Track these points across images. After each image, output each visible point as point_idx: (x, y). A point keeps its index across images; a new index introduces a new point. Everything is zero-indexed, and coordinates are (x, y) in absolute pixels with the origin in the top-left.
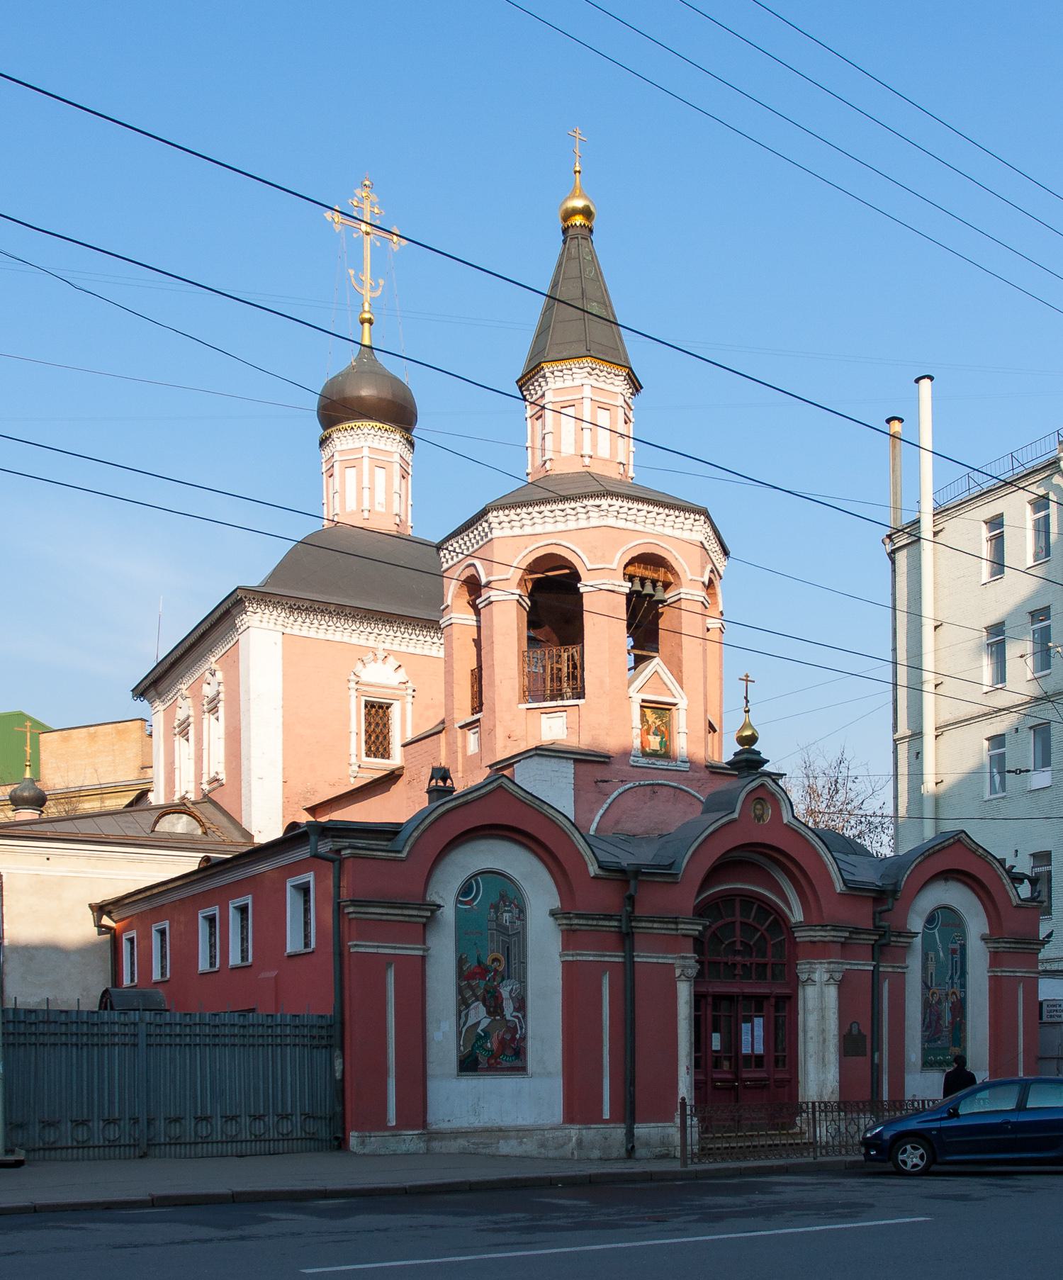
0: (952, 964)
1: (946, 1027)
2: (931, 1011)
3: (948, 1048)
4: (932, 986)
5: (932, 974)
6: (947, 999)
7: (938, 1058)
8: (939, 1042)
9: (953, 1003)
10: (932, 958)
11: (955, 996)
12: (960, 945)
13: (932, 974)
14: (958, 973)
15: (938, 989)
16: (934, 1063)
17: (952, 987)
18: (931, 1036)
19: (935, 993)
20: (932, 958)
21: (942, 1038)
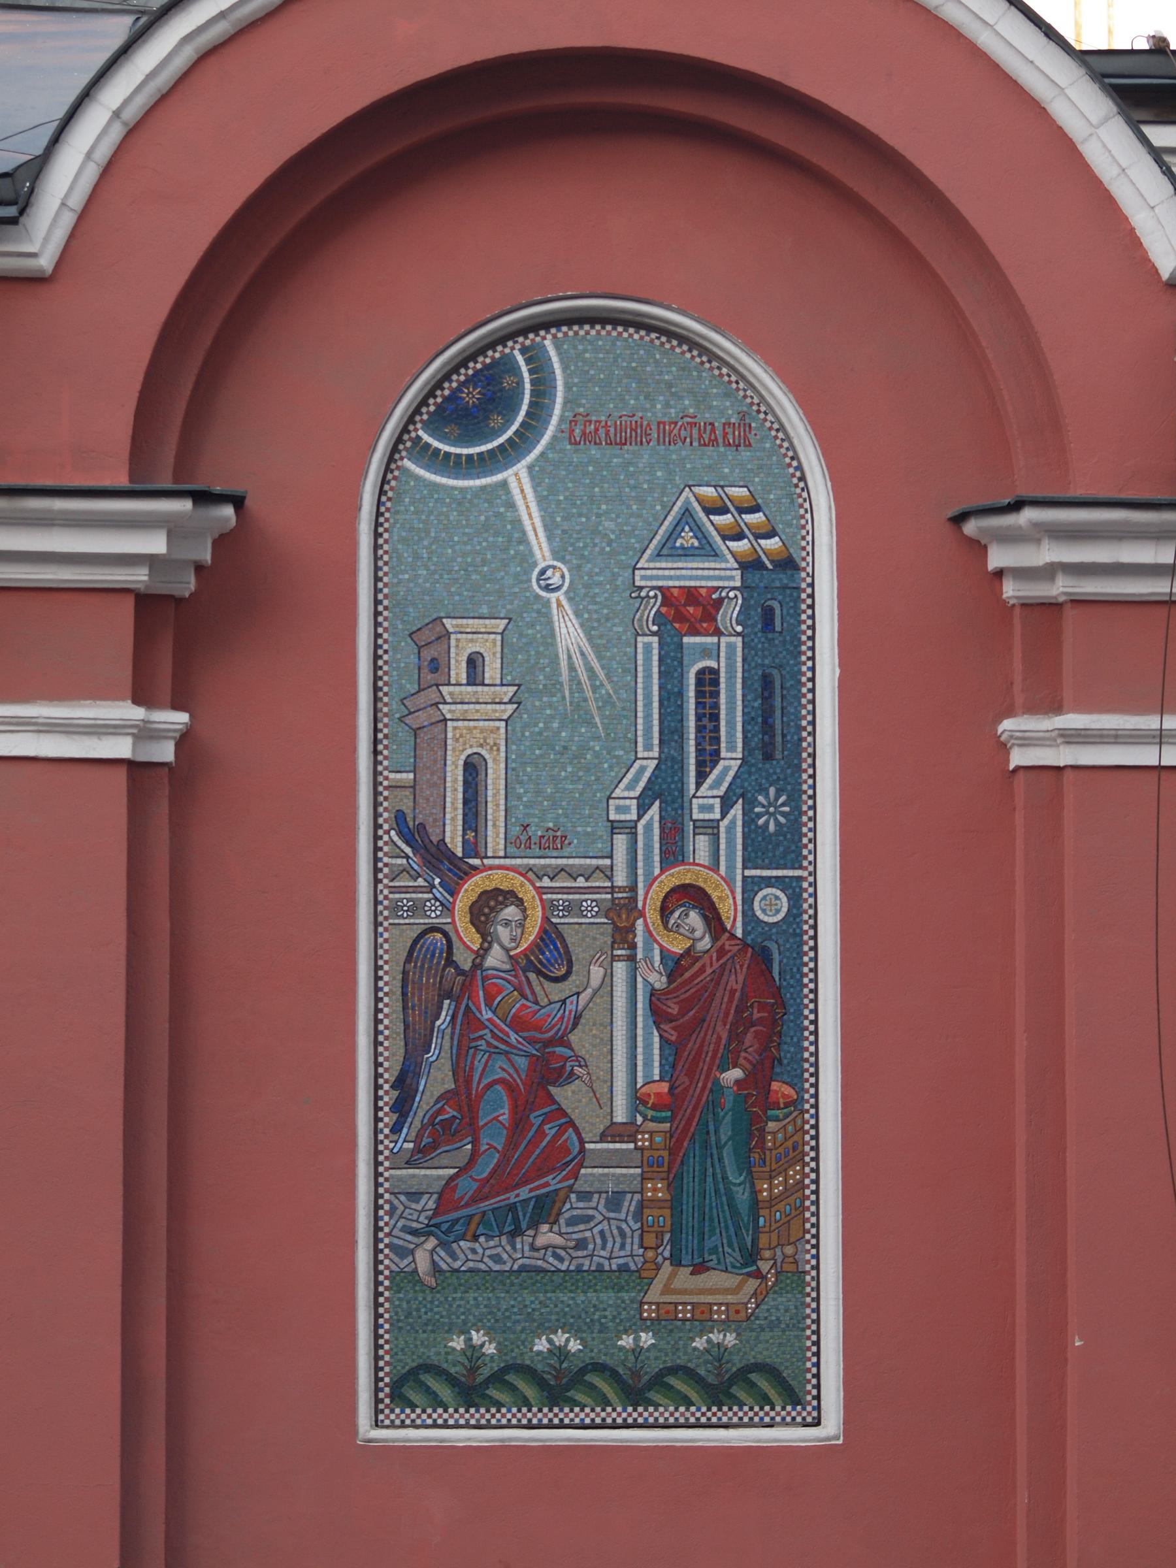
0: (671, 699)
1: (612, 1133)
2: (468, 1023)
3: (640, 1277)
4: (474, 848)
5: (473, 769)
6: (623, 936)
7: (541, 1345)
8: (546, 1236)
9: (676, 966)
10: (474, 663)
11: (694, 919)
12: (749, 565)
13: (473, 769)
14: (730, 760)
15: (524, 872)
16: (498, 1378)
17: (673, 853)
18: (467, 1187)
19: (509, 896)
20: (474, 663)
21: (574, 1206)
